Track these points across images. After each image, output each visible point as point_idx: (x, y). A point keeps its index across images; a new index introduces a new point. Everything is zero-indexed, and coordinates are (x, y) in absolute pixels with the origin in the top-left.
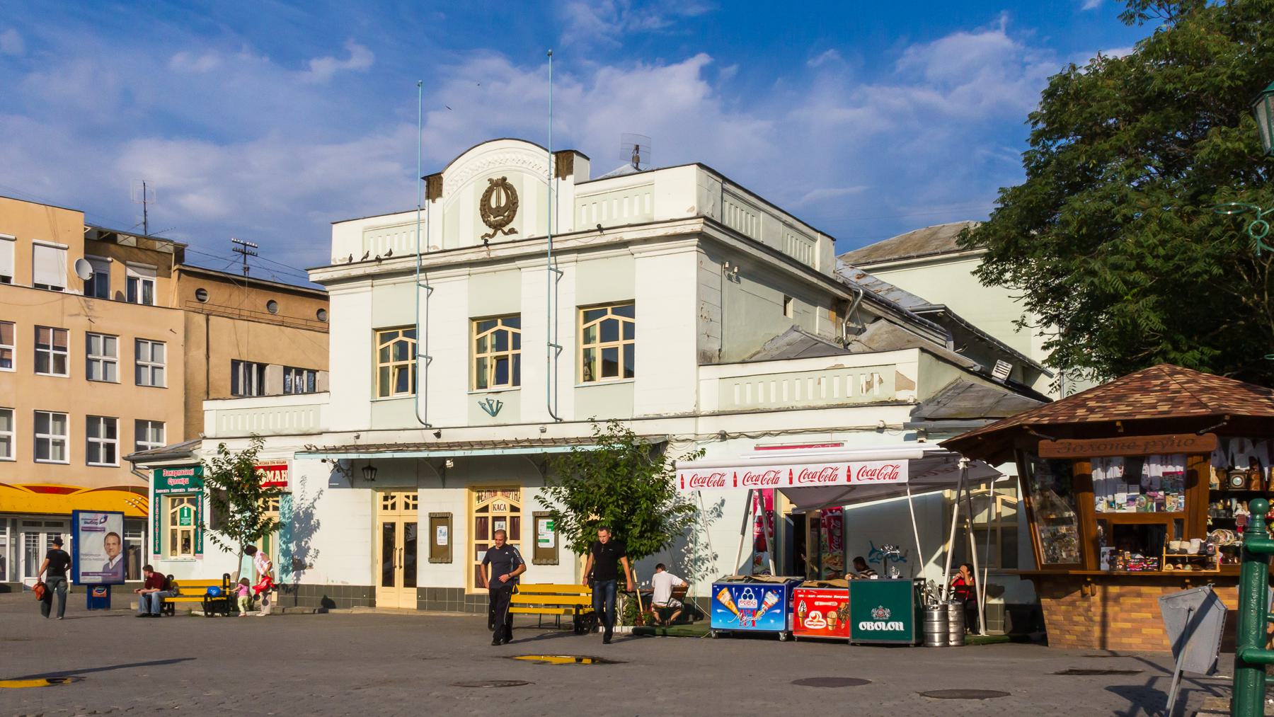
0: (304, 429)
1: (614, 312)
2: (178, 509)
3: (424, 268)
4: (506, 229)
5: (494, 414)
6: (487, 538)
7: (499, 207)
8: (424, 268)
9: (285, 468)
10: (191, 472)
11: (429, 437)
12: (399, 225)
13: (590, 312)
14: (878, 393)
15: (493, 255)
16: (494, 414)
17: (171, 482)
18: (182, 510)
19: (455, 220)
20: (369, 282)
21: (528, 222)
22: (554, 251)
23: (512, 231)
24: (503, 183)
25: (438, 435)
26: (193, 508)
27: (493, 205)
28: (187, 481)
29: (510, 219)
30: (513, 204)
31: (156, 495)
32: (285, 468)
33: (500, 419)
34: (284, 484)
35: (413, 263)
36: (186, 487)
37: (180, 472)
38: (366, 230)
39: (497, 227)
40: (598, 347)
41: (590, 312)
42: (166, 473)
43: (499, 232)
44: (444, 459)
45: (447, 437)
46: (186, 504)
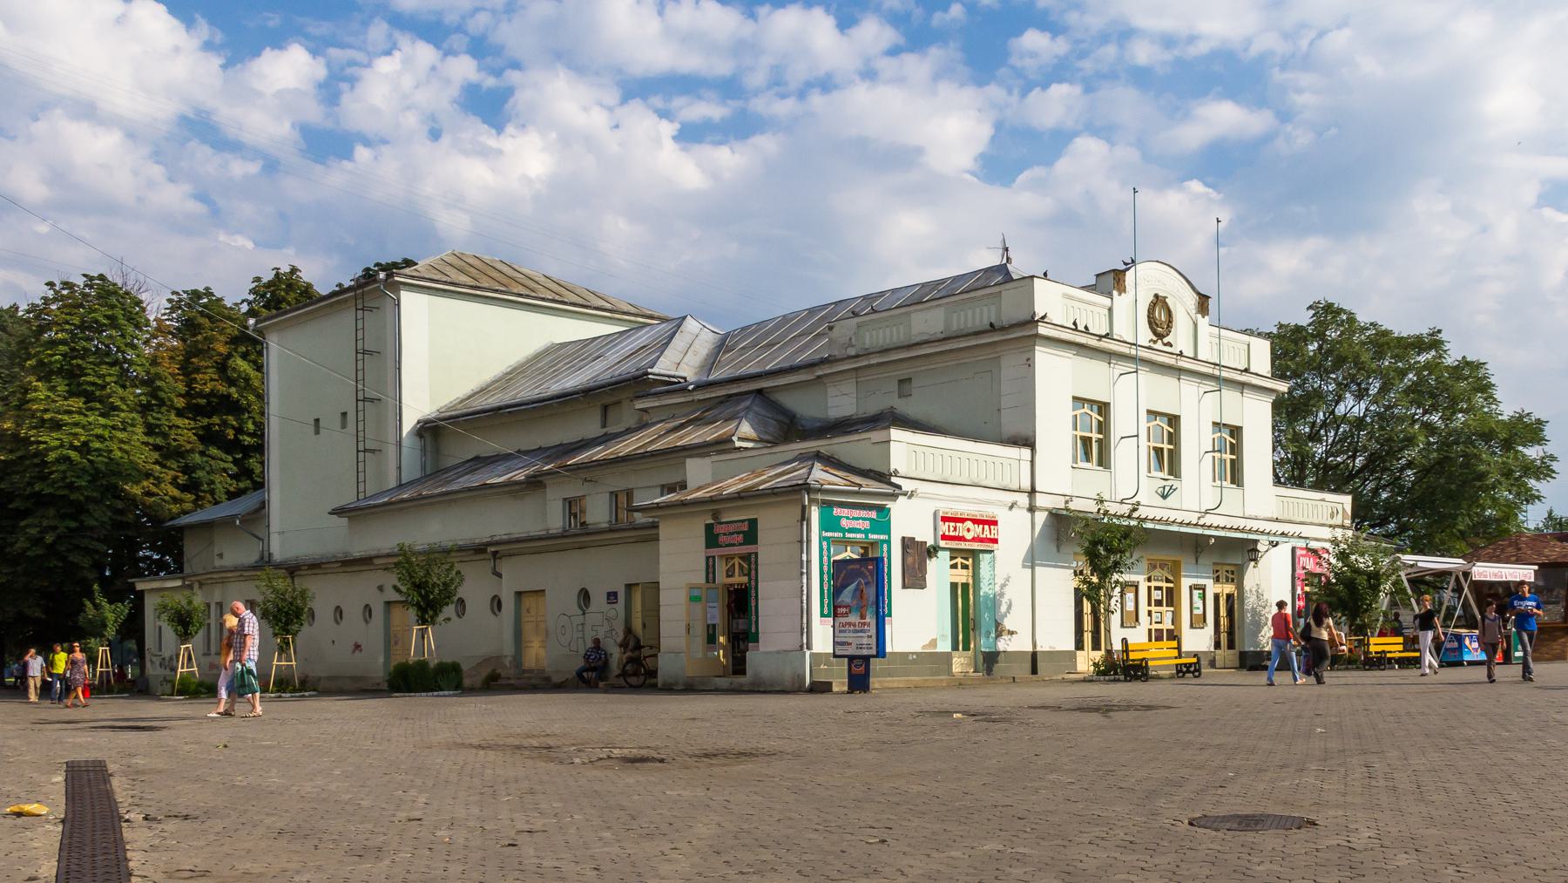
0: (1006, 483)
5: (1164, 497)
7: (1160, 318)
9: (995, 523)
10: (873, 514)
16: (1164, 497)
17: (844, 522)
21: (1180, 337)
28: (867, 525)
31: (821, 538)
32: (995, 523)
33: (1170, 501)
34: (995, 541)
35: (1124, 349)
36: (866, 532)
37: (856, 513)
39: (1160, 336)
42: (837, 511)
44: (1210, 536)
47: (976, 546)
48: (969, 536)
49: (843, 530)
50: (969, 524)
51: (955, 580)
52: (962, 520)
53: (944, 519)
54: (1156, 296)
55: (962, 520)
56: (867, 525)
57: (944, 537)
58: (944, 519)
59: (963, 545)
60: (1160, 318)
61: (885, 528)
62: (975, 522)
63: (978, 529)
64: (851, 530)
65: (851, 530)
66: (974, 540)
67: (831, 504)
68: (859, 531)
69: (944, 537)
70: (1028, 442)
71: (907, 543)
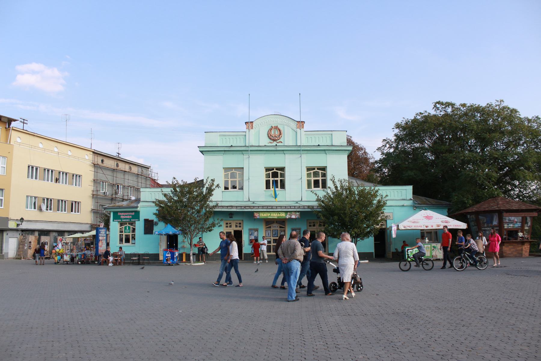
1: (318, 169)
2: (123, 227)
4: (278, 141)
7: (275, 134)
10: (133, 214)
13: (309, 169)
15: (278, 149)
18: (125, 228)
20: (223, 152)
24: (276, 128)
26: (131, 226)
27: (273, 132)
28: (131, 217)
33: (277, 199)
36: (130, 219)
37: (127, 214)
39: (274, 140)
40: (313, 179)
41: (309, 169)
43: (275, 142)
46: (128, 225)
49: (122, 219)
56: (131, 217)
60: (275, 134)
61: (138, 218)
64: (124, 219)
65: (124, 219)
67: (118, 212)
68: (128, 219)
71: (146, 221)
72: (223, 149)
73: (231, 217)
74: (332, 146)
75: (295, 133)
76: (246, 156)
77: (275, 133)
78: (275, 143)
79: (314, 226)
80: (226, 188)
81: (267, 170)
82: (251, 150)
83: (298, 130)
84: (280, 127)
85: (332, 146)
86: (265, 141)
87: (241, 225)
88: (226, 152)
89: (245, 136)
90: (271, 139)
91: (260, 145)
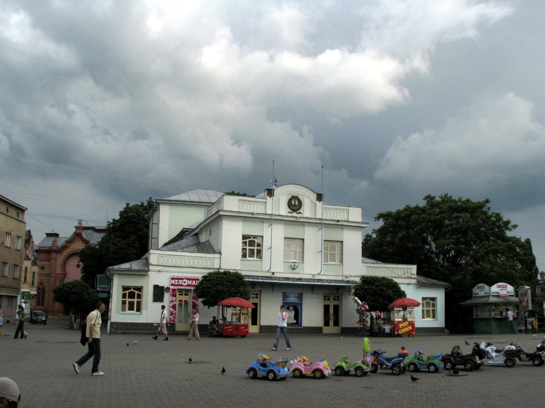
3: (271, 220)
4: (298, 212)
6: (129, 302)
7: (295, 204)
8: (271, 220)
11: (269, 275)
12: (258, 202)
14: (406, 275)
19: (278, 205)
20: (243, 219)
21: (307, 211)
22: (320, 224)
23: (300, 213)
25: (273, 273)
27: (293, 203)
29: (299, 209)
30: (300, 204)
33: (296, 271)
38: (239, 200)
43: (295, 213)
45: (274, 276)
47: (188, 288)
48: (186, 284)
50: (185, 280)
51: (180, 299)
52: (182, 279)
53: (173, 279)
54: (293, 196)
55: (182, 279)
57: (172, 285)
58: (173, 279)
59: (181, 287)
60: (295, 204)
62: (188, 279)
63: (190, 282)
66: (187, 286)
69: (172, 285)
70: (220, 253)
72: (244, 215)
73: (252, 288)
74: (348, 221)
75: (314, 205)
76: (266, 225)
77: (295, 202)
78: (294, 214)
79: (329, 299)
80: (244, 256)
81: (244, 237)
82: (274, 219)
83: (318, 202)
84: (300, 197)
85: (348, 221)
86: (284, 210)
87: (259, 296)
88: (247, 219)
89: (266, 203)
90: (290, 208)
91: (350, 220)
